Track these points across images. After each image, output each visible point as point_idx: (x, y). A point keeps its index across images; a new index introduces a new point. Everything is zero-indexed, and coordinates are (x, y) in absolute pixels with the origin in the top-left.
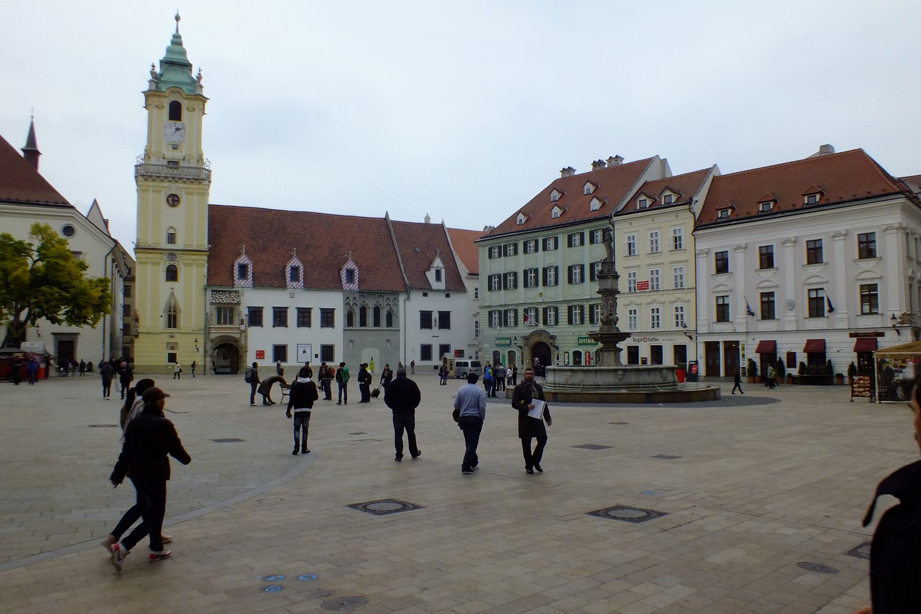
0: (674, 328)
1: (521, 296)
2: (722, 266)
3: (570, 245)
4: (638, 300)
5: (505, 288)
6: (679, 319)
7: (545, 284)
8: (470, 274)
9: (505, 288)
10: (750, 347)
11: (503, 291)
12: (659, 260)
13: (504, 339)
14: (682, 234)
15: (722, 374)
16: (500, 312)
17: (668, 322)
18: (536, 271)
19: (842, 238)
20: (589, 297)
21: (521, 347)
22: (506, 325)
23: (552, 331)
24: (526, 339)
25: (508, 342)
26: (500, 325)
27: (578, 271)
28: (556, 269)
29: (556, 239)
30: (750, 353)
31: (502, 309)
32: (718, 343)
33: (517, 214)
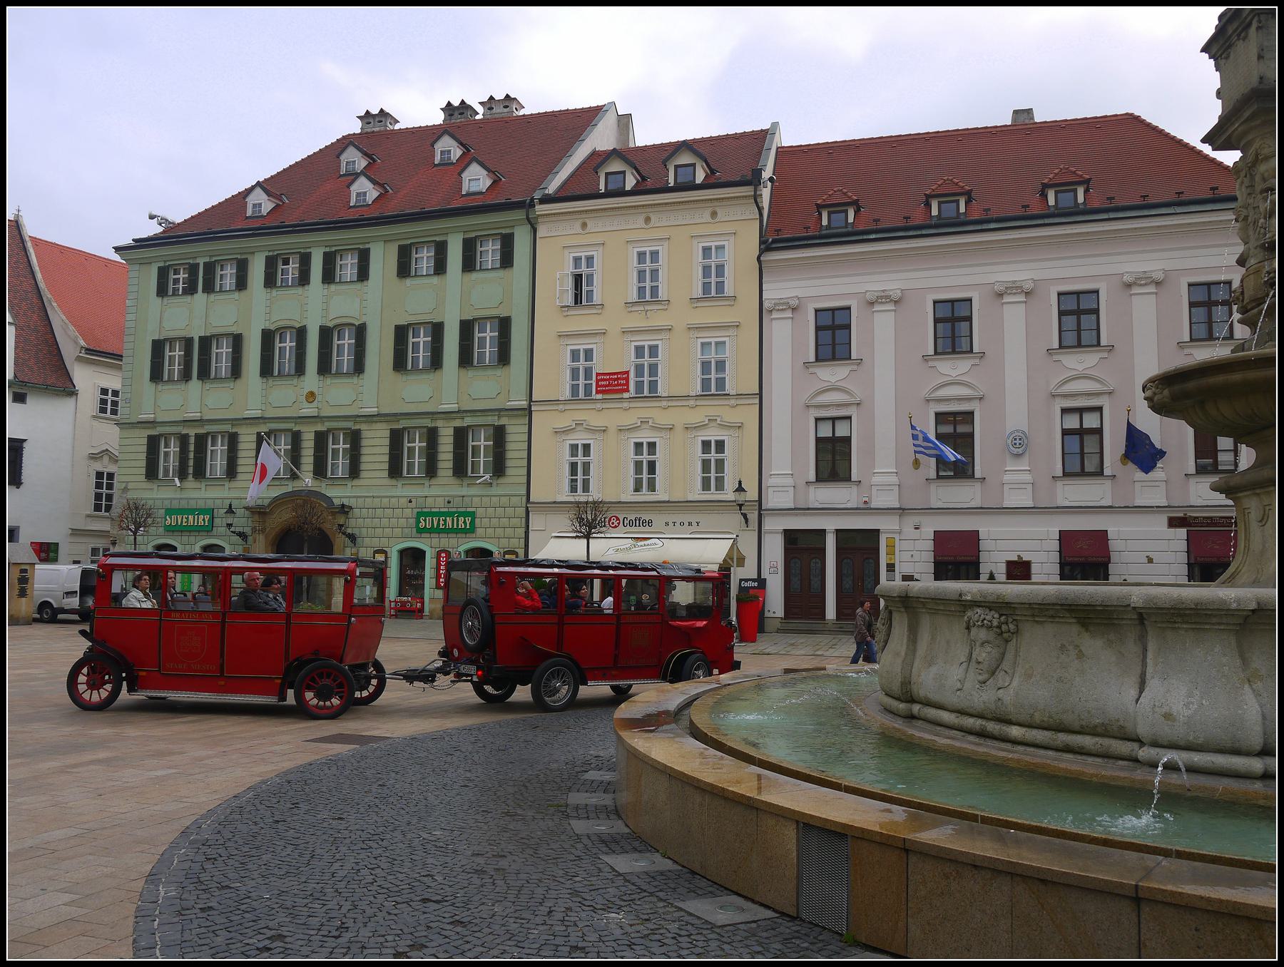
0: (696, 494)
1: (252, 397)
2: (833, 337)
3: (404, 270)
4: (596, 420)
5: (204, 374)
6: (712, 472)
7: (324, 367)
8: (89, 351)
9: (204, 374)
10: (906, 545)
11: (195, 384)
12: (659, 320)
13: (191, 511)
14: (728, 256)
15: (831, 613)
16: (184, 439)
18: (301, 333)
19: (1152, 289)
20: (454, 407)
21: (242, 535)
22: (200, 473)
23: (338, 494)
24: (259, 512)
25: (203, 520)
26: (182, 475)
27: (423, 339)
28: (360, 332)
29: (364, 257)
30: (908, 559)
31: (192, 432)
32: (822, 533)
33: (248, 191)
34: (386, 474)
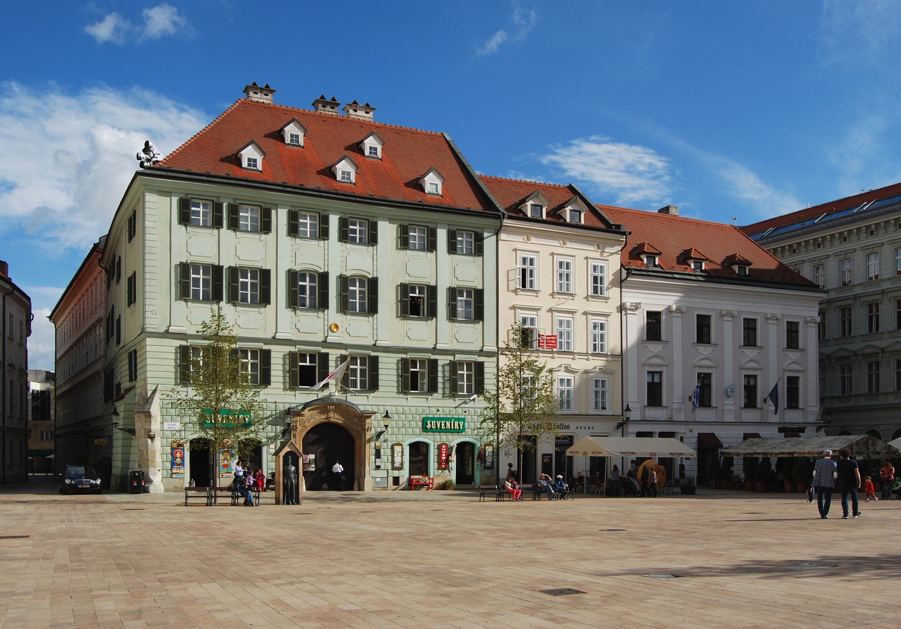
19: (775, 322)
23: (360, 401)
31: (226, 346)
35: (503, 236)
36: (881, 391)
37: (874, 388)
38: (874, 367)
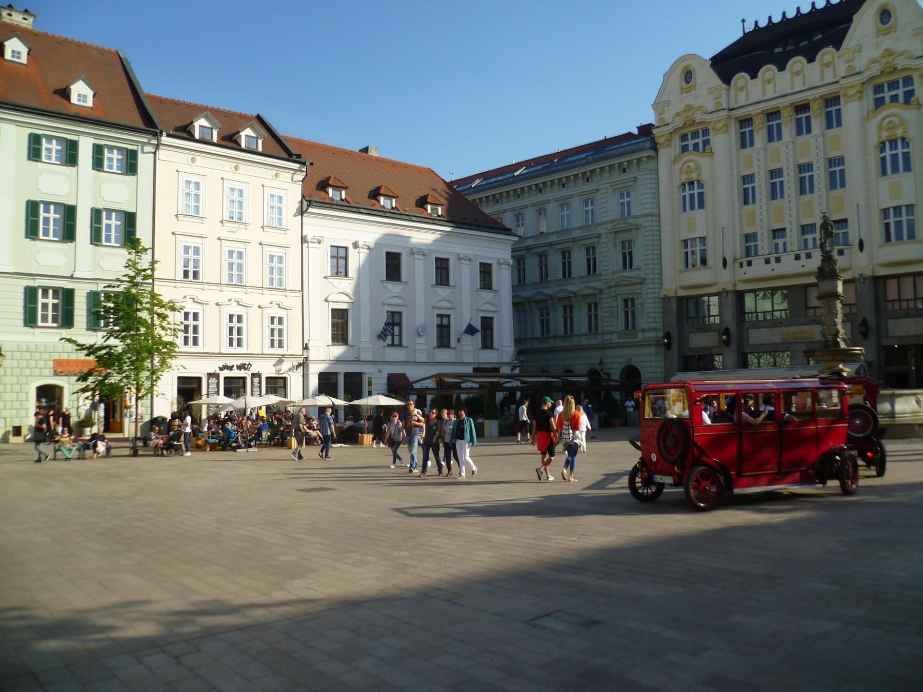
12: (241, 234)
17: (256, 338)
19: (468, 262)
34: (22, 323)
35: (162, 153)
36: (575, 332)
37: (569, 331)
38: (568, 310)
